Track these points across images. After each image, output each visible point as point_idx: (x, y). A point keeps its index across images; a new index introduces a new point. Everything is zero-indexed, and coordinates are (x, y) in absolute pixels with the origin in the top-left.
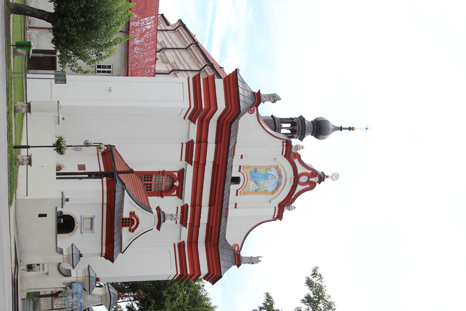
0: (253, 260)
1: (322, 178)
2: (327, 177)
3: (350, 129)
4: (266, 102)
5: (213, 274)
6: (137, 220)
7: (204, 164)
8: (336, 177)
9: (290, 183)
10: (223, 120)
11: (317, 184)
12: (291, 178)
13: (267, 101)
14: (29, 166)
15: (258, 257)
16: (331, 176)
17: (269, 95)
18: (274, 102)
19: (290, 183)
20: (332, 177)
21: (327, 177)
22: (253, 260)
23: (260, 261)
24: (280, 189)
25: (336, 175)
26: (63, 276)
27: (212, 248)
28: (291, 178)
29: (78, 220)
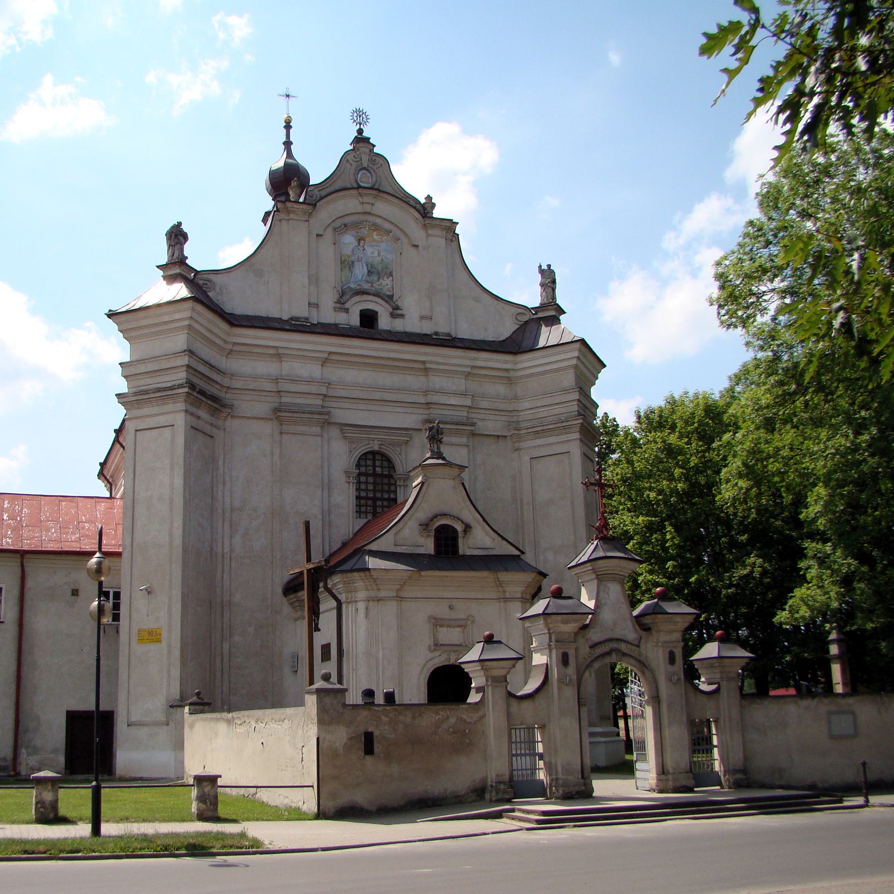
0: (548, 279)
2: (360, 131)
3: (288, 126)
4: (186, 254)
6: (435, 516)
8: (360, 116)
10: (225, 342)
11: (376, 150)
13: (182, 250)
14: (220, 782)
15: (542, 271)
16: (358, 125)
17: (170, 245)
18: (185, 237)
19: (373, 204)
20: (360, 124)
21: (360, 131)
22: (548, 279)
23: (549, 266)
24: (387, 226)
25: (355, 114)
26: (545, 687)
28: (362, 203)
29: (440, 660)
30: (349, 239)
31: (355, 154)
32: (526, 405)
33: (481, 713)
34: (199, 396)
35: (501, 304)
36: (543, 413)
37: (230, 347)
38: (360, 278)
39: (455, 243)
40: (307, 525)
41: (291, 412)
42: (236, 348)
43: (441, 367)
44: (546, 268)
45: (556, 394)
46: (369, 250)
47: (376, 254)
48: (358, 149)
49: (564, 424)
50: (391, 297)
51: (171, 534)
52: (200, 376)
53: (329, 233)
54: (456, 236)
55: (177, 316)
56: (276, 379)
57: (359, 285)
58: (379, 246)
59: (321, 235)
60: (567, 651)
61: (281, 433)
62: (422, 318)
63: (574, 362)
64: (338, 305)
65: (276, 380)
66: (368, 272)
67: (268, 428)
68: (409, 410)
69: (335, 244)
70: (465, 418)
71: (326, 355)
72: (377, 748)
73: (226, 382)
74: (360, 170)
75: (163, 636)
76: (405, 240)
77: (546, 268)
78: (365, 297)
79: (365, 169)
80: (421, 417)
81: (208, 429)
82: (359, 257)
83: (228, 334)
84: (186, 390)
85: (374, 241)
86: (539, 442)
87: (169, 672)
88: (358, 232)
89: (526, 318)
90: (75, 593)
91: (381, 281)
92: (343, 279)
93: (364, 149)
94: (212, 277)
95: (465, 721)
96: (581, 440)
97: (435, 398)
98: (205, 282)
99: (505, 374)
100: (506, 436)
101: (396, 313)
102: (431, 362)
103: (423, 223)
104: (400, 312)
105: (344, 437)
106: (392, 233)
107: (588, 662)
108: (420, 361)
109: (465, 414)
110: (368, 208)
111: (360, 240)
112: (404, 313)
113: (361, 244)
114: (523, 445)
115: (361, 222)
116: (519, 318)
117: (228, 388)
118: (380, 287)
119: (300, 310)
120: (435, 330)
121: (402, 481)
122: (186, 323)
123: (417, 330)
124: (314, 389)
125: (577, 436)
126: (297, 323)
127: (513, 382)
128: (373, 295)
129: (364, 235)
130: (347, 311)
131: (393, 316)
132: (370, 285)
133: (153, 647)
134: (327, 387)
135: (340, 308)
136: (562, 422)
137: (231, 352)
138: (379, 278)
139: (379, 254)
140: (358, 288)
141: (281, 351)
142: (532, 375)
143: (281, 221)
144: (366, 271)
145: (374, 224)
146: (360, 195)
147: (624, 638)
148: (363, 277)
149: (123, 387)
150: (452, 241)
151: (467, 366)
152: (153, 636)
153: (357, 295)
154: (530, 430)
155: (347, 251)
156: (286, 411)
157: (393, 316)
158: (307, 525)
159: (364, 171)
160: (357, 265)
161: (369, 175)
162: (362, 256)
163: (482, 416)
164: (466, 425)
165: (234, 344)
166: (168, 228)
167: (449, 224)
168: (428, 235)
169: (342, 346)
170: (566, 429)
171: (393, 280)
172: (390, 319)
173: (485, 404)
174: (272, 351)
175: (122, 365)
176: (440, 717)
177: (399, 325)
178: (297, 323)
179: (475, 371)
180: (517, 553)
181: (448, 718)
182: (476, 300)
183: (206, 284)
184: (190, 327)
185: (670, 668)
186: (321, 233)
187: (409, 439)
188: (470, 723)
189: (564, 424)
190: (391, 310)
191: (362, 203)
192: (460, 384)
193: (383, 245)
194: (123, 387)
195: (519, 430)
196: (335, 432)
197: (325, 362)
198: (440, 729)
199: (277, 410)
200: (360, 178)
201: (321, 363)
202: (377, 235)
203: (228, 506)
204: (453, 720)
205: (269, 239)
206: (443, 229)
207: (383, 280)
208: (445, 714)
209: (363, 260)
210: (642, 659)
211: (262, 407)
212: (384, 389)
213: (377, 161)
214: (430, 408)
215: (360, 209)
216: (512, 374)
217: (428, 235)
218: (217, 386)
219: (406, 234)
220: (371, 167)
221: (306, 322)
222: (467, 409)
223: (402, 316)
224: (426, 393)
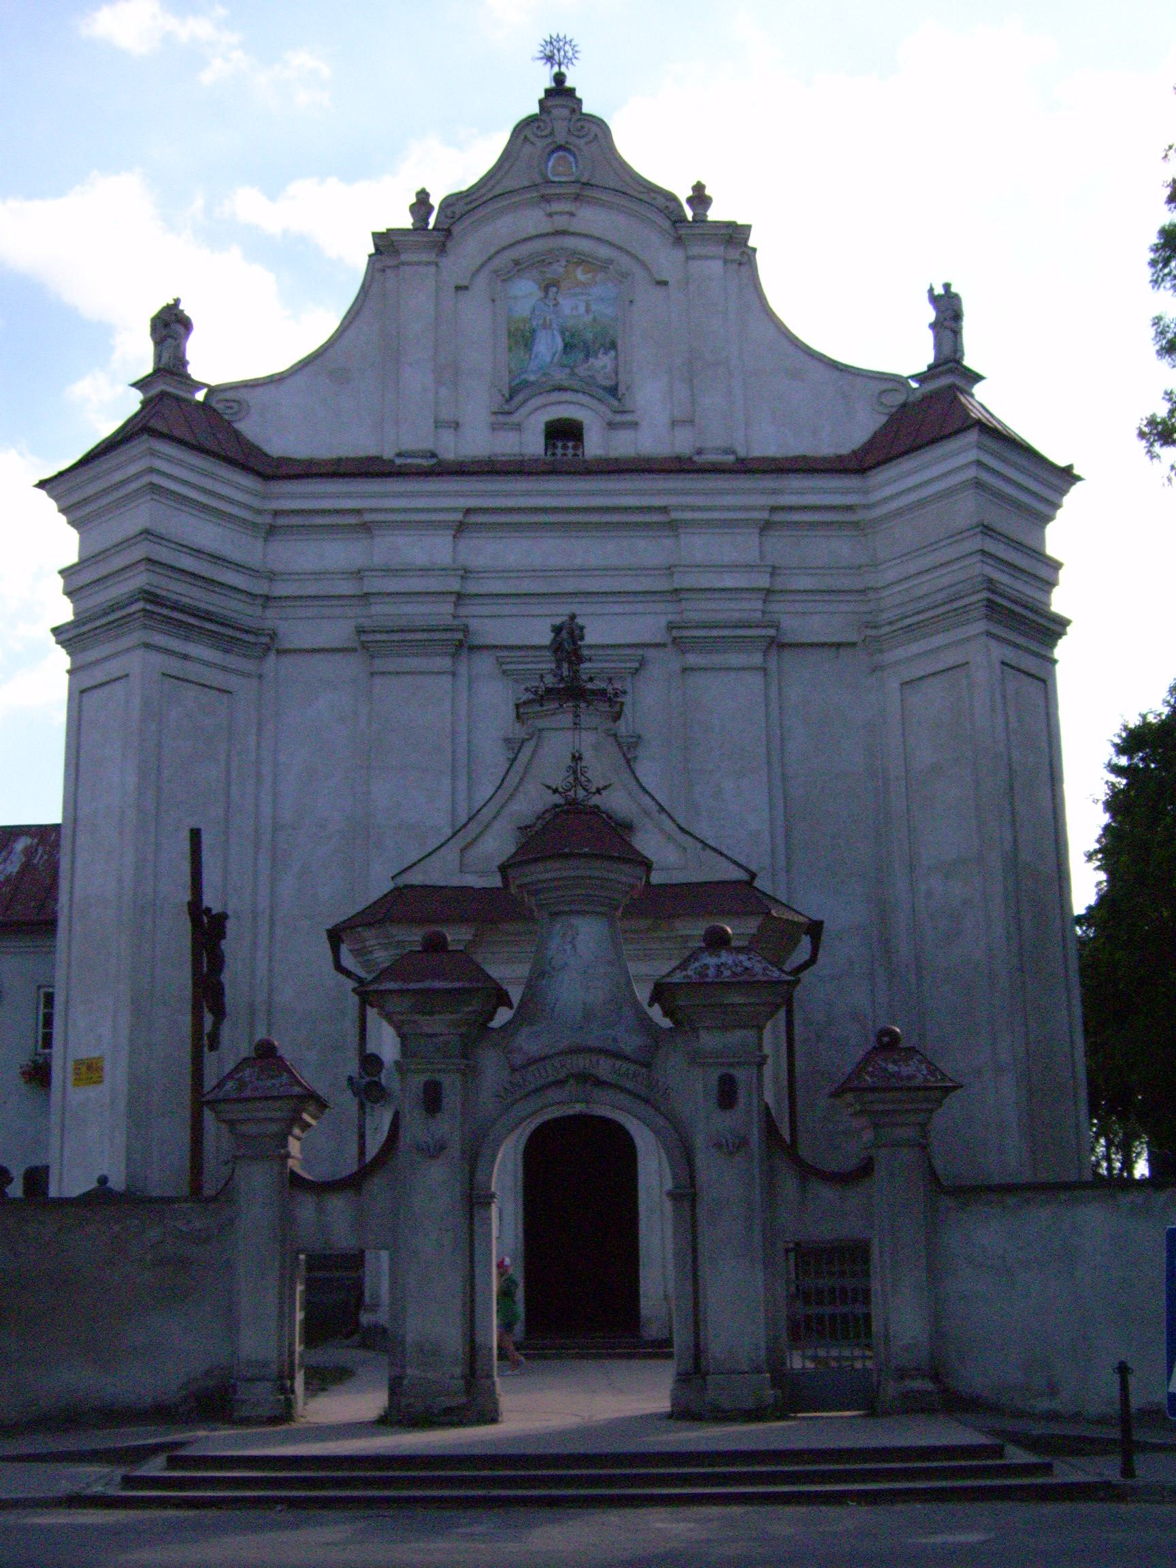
2: (559, 78)
5: (979, 464)
7: (462, 572)
9: (572, 214)
10: (259, 512)
12: (550, 215)
15: (934, 299)
18: (186, 324)
19: (572, 214)
20: (560, 65)
21: (559, 78)
23: (947, 287)
24: (604, 252)
28: (550, 215)
30: (526, 290)
32: (890, 575)
37: (268, 520)
38: (548, 359)
42: (281, 521)
43: (698, 515)
46: (566, 305)
47: (582, 309)
52: (188, 580)
53: (482, 280)
57: (545, 374)
59: (466, 288)
61: (372, 674)
62: (674, 423)
64: (501, 418)
65: (358, 574)
66: (566, 346)
68: (640, 608)
69: (493, 301)
70: (759, 615)
71: (459, 517)
74: (553, 152)
76: (640, 273)
79: (560, 148)
80: (663, 621)
83: (265, 497)
85: (579, 284)
86: (914, 648)
91: (591, 360)
94: (243, 394)
98: (231, 404)
100: (854, 645)
101: (622, 419)
102: (683, 508)
105: (504, 672)
109: (759, 605)
110: (561, 222)
111: (548, 287)
113: (551, 295)
114: (889, 657)
117: (267, 598)
124: (434, 584)
130: (518, 427)
138: (587, 357)
139: (588, 311)
141: (368, 517)
142: (899, 513)
143: (383, 271)
145: (574, 253)
146: (546, 199)
149: (65, 612)
150: (740, 264)
151: (762, 508)
159: (561, 153)
161: (571, 159)
165: (277, 513)
166: (154, 310)
168: (688, 258)
169: (494, 494)
171: (616, 358)
173: (804, 583)
174: (353, 520)
177: (623, 445)
179: (778, 517)
186: (464, 283)
187: (636, 665)
193: (596, 291)
194: (65, 612)
195: (875, 627)
197: (460, 529)
199: (360, 631)
200: (553, 167)
201: (453, 532)
202: (585, 272)
209: (554, 326)
211: (337, 631)
212: (583, 571)
214: (680, 600)
215: (547, 227)
217: (688, 258)
219: (643, 264)
223: (634, 425)
224: (670, 570)
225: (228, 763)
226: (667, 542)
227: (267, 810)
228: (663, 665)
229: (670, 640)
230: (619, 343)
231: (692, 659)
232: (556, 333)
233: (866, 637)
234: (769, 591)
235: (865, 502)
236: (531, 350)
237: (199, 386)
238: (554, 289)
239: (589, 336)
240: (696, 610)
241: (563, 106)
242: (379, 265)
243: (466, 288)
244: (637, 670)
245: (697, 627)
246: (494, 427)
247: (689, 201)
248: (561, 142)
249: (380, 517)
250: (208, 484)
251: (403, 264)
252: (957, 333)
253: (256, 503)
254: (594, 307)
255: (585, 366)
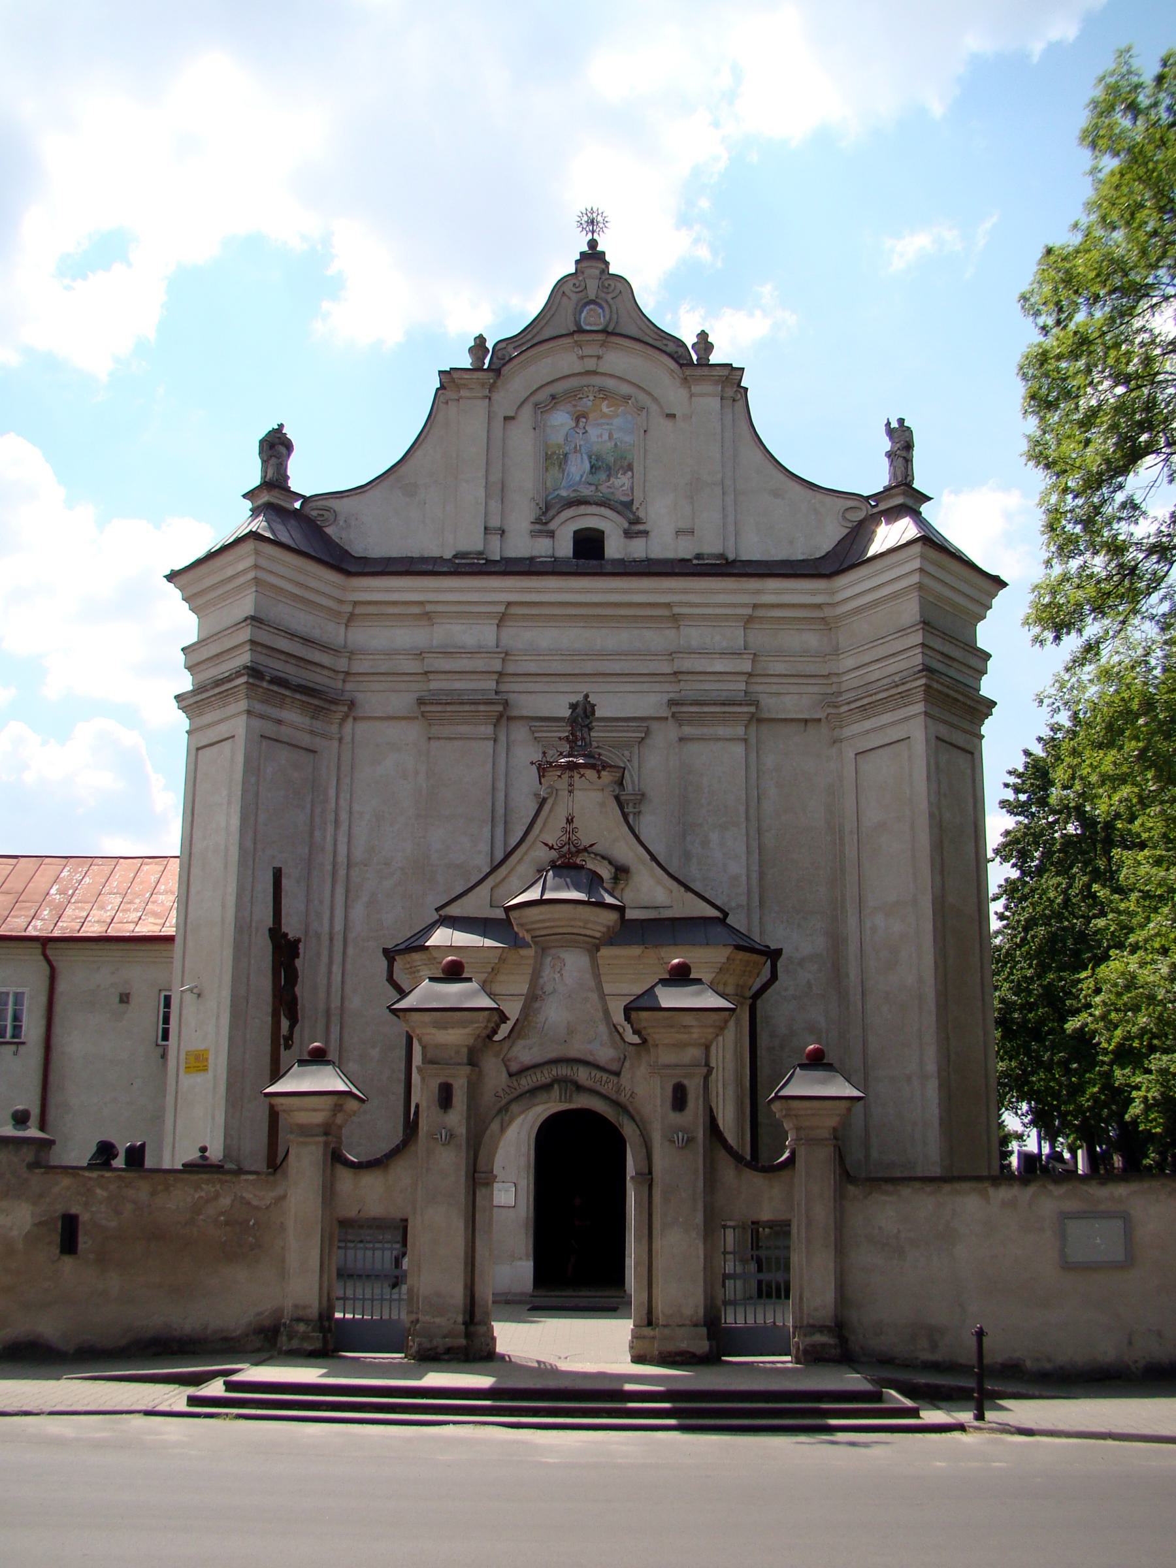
1: (593, 257)
2: (593, 244)
7: (502, 655)
9: (599, 357)
10: (341, 602)
12: (582, 358)
15: (890, 432)
18: (288, 446)
21: (593, 244)
23: (901, 421)
24: (625, 389)
27: (839, 597)
30: (561, 419)
31: (575, 281)
32: (850, 663)
33: (279, 1191)
34: (275, 688)
35: (819, 496)
36: (876, 673)
37: (349, 609)
38: (578, 479)
39: (741, 403)
40: (278, 875)
41: (440, 704)
42: (358, 611)
44: (897, 426)
45: (890, 638)
46: (593, 432)
47: (606, 437)
48: (583, 273)
49: (900, 689)
50: (628, 505)
51: (223, 906)
53: (527, 412)
54: (742, 391)
55: (241, 567)
56: (421, 654)
58: (612, 424)
59: (512, 418)
60: (450, 1081)
61: (430, 738)
62: (678, 532)
63: (916, 578)
64: (538, 527)
65: (420, 655)
66: (592, 467)
67: (412, 732)
68: (645, 687)
70: (742, 694)
71: (502, 609)
72: (84, 1242)
73: (342, 664)
75: (210, 1061)
76: (654, 408)
77: (897, 426)
78: (583, 509)
80: (666, 697)
81: (305, 740)
82: (576, 447)
84: (243, 679)
85: (604, 416)
86: (868, 725)
87: (213, 1118)
88: (575, 406)
89: (861, 515)
90: (125, 998)
91: (612, 479)
92: (549, 484)
93: (593, 270)
94: (331, 503)
95: (249, 1203)
96: (926, 714)
97: (687, 664)
98: (321, 512)
99: (817, 614)
100: (819, 720)
101: (635, 529)
102: (681, 604)
103: (681, 376)
104: (641, 527)
105: (535, 738)
106: (633, 399)
107: (504, 1102)
108: (664, 604)
109: (743, 686)
110: (591, 364)
112: (648, 529)
113: (581, 425)
114: (847, 732)
115: (580, 389)
116: (849, 516)
117: (347, 673)
118: (612, 490)
119: (470, 540)
120: (697, 551)
121: (631, 805)
122: (251, 575)
123: (670, 555)
124: (479, 664)
125: (920, 707)
126: (463, 561)
127: (833, 625)
128: (597, 504)
129: (585, 409)
130: (551, 534)
131: (628, 534)
132: (593, 488)
133: (199, 1078)
134: (503, 660)
135: (540, 531)
136: (897, 686)
137: (352, 617)
138: (609, 476)
139: (610, 437)
140: (573, 495)
141: (429, 608)
142: (858, 611)
144: (587, 466)
145: (601, 390)
147: (590, 1058)
148: (582, 476)
149: (186, 683)
150: (734, 400)
152: (198, 1063)
153: (570, 507)
154: (853, 706)
155: (557, 438)
156: (432, 703)
157: (628, 534)
158: (278, 875)
159: (592, 306)
160: (572, 458)
161: (600, 311)
162: (582, 443)
163: (774, 688)
164: (740, 705)
165: (356, 603)
167: (726, 372)
168: (691, 396)
169: (529, 590)
170: (904, 698)
171: (633, 477)
172: (623, 540)
173: (779, 667)
174: (416, 610)
175: (186, 651)
176: (203, 1194)
177: (638, 549)
178: (463, 561)
179: (760, 613)
180: (716, 913)
181: (217, 1196)
182: (776, 493)
183: (323, 515)
184: (257, 581)
185: (675, 1118)
186: (512, 414)
187: (643, 735)
188: (257, 1208)
189: (900, 689)
190: (626, 525)
191: (582, 358)
192: (734, 636)
193: (617, 421)
195: (836, 707)
196: (520, 733)
197: (502, 620)
198: (201, 1217)
199: (421, 702)
201: (497, 622)
203: (342, 858)
204: (225, 1201)
205: (428, 434)
206: (716, 383)
207: (617, 478)
208: (213, 1189)
209: (583, 450)
210: (623, 1099)
211: (401, 701)
212: (601, 655)
213: (613, 286)
214: (680, 681)
215: (578, 367)
216: (827, 612)
217: (691, 396)
218: (326, 672)
219: (655, 400)
220: (601, 299)
221: (478, 559)
222: (744, 678)
223: (646, 533)
224: (671, 655)
225: (312, 811)
226: (667, 632)
227: (342, 850)
228: (664, 735)
229: (670, 715)
230: (635, 465)
231: (687, 730)
232: (585, 457)
233: (828, 714)
234: (750, 675)
235: (830, 601)
236: (563, 471)
237: (298, 496)
238: (584, 420)
239: (611, 460)
240: (690, 688)
241: (596, 268)
242: (442, 399)
243: (512, 418)
244: (643, 739)
245: (691, 704)
246: (534, 534)
247: (693, 346)
248: (592, 296)
249: (440, 608)
250: (301, 578)
251: (461, 398)
252: (908, 461)
253: (336, 593)
254: (615, 436)
255: (608, 484)
